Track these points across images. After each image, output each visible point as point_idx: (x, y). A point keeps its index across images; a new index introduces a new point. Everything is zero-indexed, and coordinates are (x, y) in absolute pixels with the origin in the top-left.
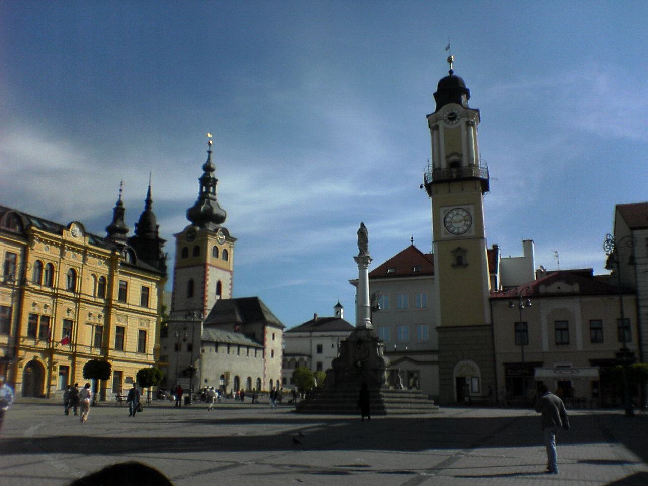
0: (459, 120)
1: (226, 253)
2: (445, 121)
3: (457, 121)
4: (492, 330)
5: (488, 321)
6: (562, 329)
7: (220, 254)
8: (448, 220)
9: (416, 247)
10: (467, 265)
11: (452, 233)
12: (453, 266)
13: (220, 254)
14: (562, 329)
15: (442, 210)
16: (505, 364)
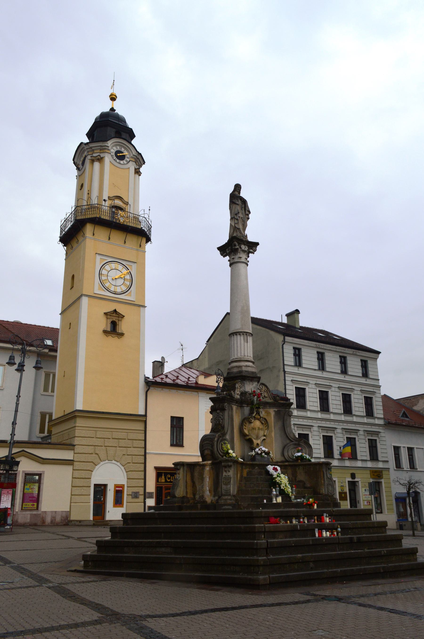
2: (112, 156)
3: (125, 162)
4: (145, 422)
5: (142, 412)
8: (104, 272)
10: (122, 335)
11: (108, 290)
12: (105, 332)
15: (98, 257)
16: (156, 468)
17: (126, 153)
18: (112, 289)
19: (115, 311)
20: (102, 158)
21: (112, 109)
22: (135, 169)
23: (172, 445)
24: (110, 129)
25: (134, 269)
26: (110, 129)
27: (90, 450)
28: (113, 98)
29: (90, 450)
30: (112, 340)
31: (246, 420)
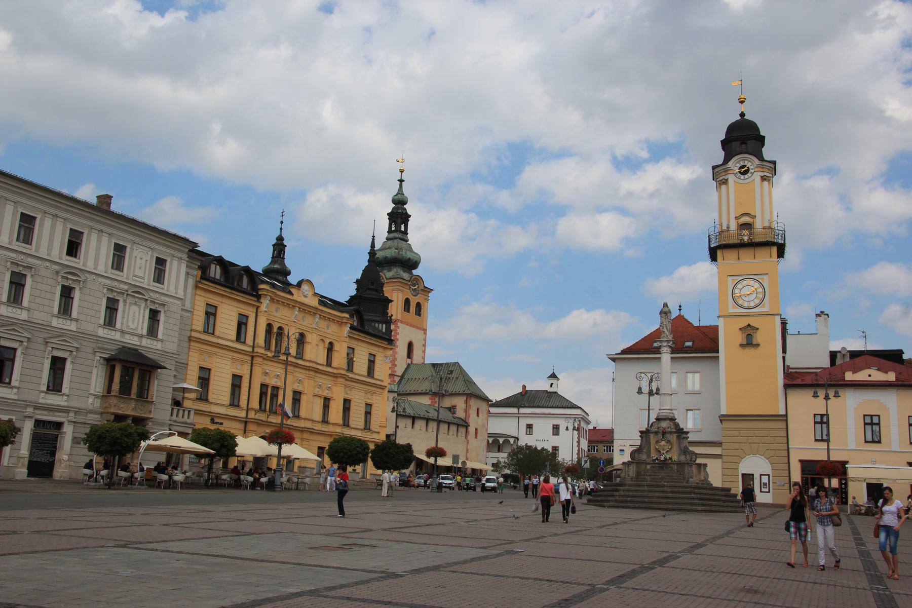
0: (752, 174)
1: (419, 306)
4: (787, 420)
5: (783, 412)
6: (872, 423)
7: (413, 308)
9: (686, 317)
10: (758, 345)
12: (741, 345)
13: (413, 308)
14: (872, 423)
15: (730, 279)
17: (748, 164)
18: (746, 305)
19: (749, 325)
20: (727, 180)
22: (762, 177)
25: (765, 280)
30: (749, 351)
31: (657, 442)
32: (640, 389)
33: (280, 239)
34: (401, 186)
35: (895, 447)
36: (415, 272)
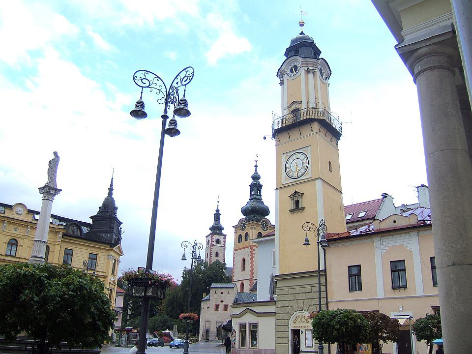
6: (398, 269)
8: (288, 165)
10: (303, 208)
12: (291, 211)
14: (398, 269)
15: (284, 156)
17: (296, 64)
21: (302, 33)
23: (393, 288)
24: (303, 50)
26: (303, 50)
27: (286, 304)
28: (302, 25)
29: (286, 304)
30: (298, 215)
32: (184, 256)
33: (218, 211)
34: (256, 168)
35: (420, 293)
36: (266, 217)
